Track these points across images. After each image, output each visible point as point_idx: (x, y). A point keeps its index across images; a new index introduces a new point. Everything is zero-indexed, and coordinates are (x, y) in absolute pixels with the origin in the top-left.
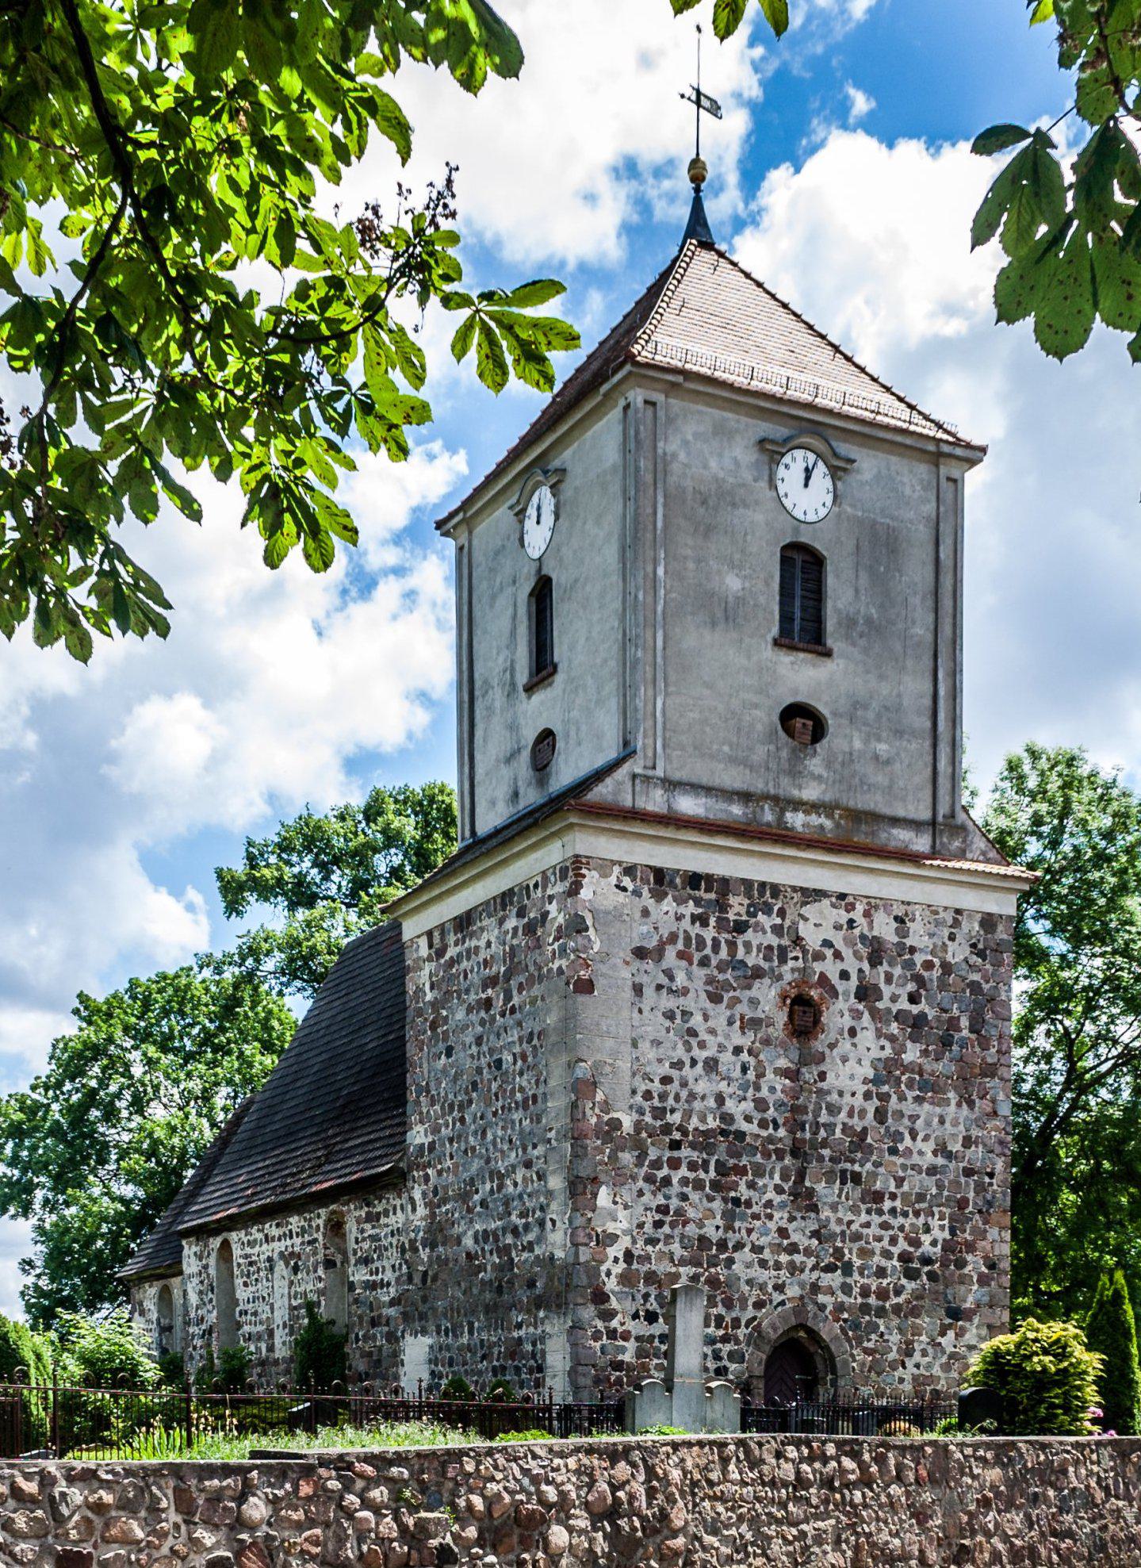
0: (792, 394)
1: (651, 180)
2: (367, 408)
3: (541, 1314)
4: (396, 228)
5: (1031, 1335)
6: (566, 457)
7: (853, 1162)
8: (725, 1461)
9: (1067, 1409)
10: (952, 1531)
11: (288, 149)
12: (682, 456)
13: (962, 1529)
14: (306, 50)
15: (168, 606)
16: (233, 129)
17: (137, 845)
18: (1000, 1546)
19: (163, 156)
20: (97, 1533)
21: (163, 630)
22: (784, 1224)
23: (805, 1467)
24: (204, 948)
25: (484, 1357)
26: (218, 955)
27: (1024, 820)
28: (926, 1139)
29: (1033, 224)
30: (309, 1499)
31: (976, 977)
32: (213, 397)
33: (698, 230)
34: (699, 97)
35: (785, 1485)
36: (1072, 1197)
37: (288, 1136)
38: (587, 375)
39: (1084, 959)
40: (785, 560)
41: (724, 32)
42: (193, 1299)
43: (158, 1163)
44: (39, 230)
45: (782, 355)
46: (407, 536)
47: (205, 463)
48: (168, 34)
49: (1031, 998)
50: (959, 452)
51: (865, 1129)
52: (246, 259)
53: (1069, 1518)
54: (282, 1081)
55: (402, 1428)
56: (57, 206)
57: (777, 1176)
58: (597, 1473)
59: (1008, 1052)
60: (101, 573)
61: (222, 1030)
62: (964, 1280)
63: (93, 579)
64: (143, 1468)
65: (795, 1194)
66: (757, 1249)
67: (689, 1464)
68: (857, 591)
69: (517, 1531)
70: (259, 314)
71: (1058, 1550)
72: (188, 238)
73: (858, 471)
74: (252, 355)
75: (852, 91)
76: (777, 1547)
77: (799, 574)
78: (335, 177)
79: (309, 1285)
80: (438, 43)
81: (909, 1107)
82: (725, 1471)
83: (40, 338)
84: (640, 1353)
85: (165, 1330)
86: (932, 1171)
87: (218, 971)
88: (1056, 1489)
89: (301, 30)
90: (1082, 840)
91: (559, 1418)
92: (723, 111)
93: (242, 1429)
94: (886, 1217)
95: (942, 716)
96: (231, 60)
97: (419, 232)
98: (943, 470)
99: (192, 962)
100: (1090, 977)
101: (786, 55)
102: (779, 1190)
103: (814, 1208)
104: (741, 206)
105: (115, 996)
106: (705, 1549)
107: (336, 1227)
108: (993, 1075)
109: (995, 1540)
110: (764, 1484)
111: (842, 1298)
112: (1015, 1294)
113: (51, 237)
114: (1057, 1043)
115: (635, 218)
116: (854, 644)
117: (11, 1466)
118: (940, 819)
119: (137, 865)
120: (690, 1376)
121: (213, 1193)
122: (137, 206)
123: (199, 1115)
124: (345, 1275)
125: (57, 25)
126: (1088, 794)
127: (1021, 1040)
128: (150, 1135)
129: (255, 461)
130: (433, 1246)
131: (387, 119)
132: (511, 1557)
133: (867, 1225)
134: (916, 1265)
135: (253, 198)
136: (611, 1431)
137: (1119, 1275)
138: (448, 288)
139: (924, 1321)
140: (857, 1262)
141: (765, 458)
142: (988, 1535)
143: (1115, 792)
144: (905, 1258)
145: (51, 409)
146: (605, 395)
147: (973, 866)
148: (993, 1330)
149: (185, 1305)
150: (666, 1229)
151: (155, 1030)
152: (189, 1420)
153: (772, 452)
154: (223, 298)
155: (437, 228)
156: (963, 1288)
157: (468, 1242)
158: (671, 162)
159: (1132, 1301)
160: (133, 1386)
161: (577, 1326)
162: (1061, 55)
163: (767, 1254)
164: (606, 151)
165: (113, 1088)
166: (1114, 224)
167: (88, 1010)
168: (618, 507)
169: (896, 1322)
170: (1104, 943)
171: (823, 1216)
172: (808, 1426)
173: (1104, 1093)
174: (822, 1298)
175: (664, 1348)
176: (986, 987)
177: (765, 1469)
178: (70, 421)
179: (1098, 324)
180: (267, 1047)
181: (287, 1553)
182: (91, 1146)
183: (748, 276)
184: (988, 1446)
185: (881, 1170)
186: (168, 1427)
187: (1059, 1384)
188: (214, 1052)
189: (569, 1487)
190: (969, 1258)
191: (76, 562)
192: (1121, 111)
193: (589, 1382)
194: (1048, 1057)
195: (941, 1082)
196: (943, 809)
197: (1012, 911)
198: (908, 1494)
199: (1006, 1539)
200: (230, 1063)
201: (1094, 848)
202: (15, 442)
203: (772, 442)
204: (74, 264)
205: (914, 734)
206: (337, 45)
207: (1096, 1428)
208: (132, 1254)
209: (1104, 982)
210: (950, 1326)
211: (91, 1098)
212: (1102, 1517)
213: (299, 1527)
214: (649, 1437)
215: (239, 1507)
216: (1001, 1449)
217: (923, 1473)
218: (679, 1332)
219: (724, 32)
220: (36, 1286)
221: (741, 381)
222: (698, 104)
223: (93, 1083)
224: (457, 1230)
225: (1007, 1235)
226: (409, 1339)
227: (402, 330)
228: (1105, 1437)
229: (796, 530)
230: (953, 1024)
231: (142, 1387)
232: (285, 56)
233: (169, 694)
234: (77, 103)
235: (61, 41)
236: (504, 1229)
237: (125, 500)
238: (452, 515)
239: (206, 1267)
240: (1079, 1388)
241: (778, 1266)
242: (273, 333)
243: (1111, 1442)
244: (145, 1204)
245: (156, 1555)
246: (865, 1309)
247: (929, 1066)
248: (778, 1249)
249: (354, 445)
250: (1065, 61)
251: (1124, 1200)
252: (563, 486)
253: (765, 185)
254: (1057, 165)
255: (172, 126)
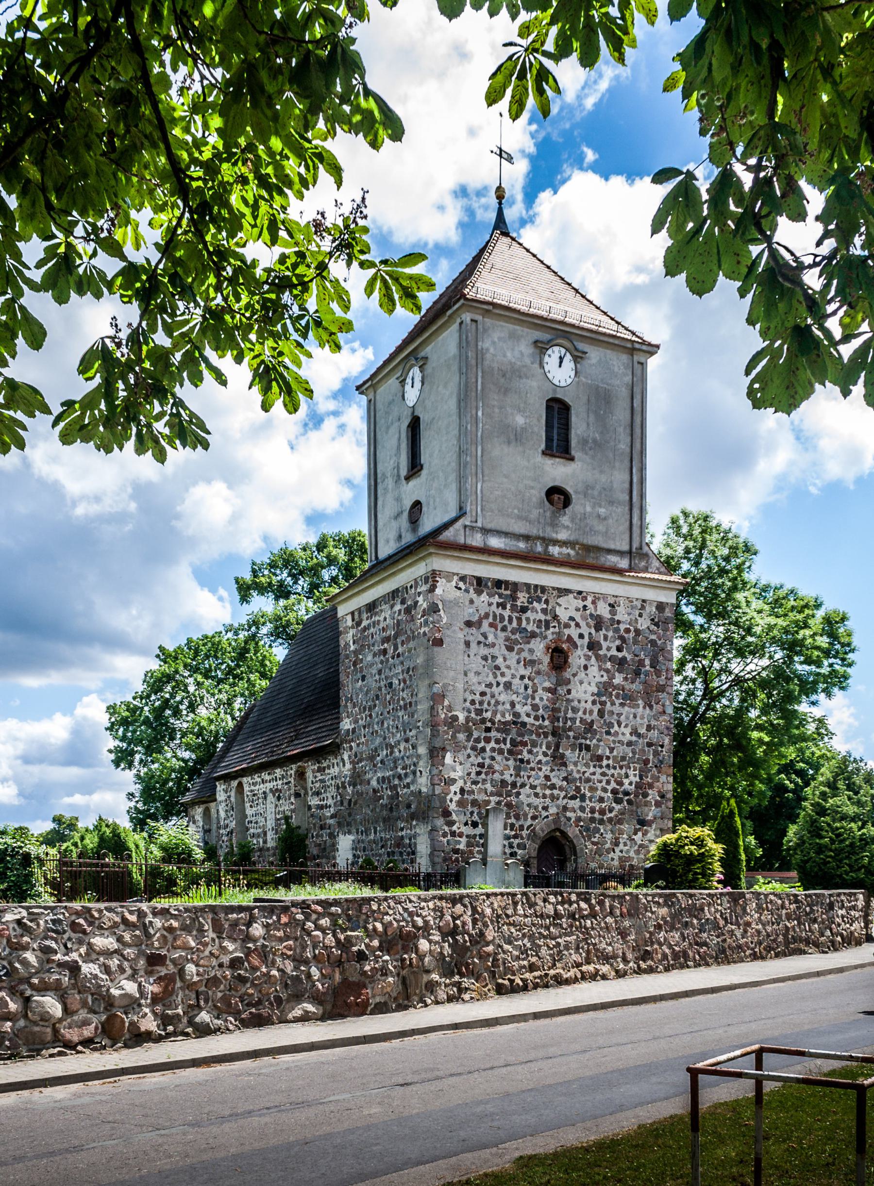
0: (552, 316)
1: (475, 198)
2: (318, 324)
3: (414, 823)
4: (334, 225)
5: (684, 834)
6: (428, 351)
7: (586, 739)
8: (515, 904)
9: (704, 875)
10: (640, 942)
11: (275, 181)
12: (492, 350)
13: (646, 941)
14: (285, 126)
15: (208, 433)
16: (244, 170)
17: (191, 564)
18: (667, 951)
19: (206, 185)
20: (169, 944)
21: (206, 446)
22: (548, 773)
23: (559, 907)
24: (228, 621)
25: (382, 847)
26: (236, 625)
27: (680, 551)
28: (626, 726)
29: (685, 222)
30: (286, 924)
31: (654, 637)
32: (233, 318)
33: (501, 226)
34: (501, 153)
35: (549, 917)
36: (707, 758)
37: (275, 725)
38: (439, 306)
39: (713, 627)
40: (548, 408)
41: (515, 116)
42: (222, 814)
43: (203, 740)
44: (137, 226)
45: (547, 294)
46: (340, 394)
47: (229, 353)
48: (209, 118)
49: (684, 648)
50: (644, 348)
51: (592, 721)
52: (251, 242)
53: (705, 935)
54: (272, 694)
55: (337, 886)
56: (147, 212)
57: (544, 747)
58: (445, 910)
59: (671, 678)
60: (171, 415)
61: (238, 666)
62: (648, 804)
63: (167, 418)
64: (195, 907)
65: (554, 757)
66: (533, 787)
67: (496, 905)
68: (588, 424)
69: (401, 942)
70: (259, 272)
71: (699, 953)
72: (219, 230)
73: (589, 358)
74: (254, 294)
75: (585, 149)
76: (544, 951)
77: (556, 415)
78: (301, 197)
79: (286, 807)
80: (357, 122)
81: (617, 709)
82: (515, 909)
83: (138, 285)
84: (469, 844)
85: (207, 831)
86: (630, 744)
87: (236, 634)
88: (698, 919)
89: (281, 115)
90: (712, 562)
91: (424, 880)
92: (514, 160)
93: (249, 886)
94: (604, 770)
95: (635, 493)
96: (243, 132)
97: (347, 227)
98: (636, 358)
99: (222, 629)
100: (717, 637)
101: (549, 129)
102: (545, 754)
103: (565, 764)
104: (524, 212)
105: (179, 648)
106: (504, 952)
107: (301, 775)
108: (663, 691)
109: (664, 947)
110: (537, 916)
111: (580, 814)
112: (675, 812)
113: (144, 229)
114: (699, 673)
115: (466, 219)
116: (586, 454)
117: (122, 907)
118: (634, 550)
119: (191, 576)
120: (496, 857)
121: (234, 756)
122: (191, 212)
123: (226, 713)
124: (306, 801)
125: (147, 112)
126: (715, 536)
127: (678, 672)
128: (199, 724)
129: (256, 353)
130: (354, 785)
131: (329, 165)
132: (398, 957)
133: (594, 774)
134: (620, 796)
135: (255, 207)
136: (453, 887)
137: (733, 802)
138: (363, 257)
139: (625, 827)
140: (588, 794)
141: (538, 351)
142: (660, 944)
143: (730, 535)
144: (614, 792)
145: (144, 324)
146: (450, 316)
147: (652, 576)
148: (663, 832)
149: (218, 818)
150: (483, 776)
151: (201, 666)
152: (220, 881)
153: (541, 348)
154: (239, 263)
155: (357, 224)
156: (646, 809)
157: (374, 783)
158: (486, 188)
159: (740, 815)
160: (189, 863)
161: (434, 830)
162: (701, 129)
163: (538, 790)
164: (449, 182)
165: (178, 698)
166: (730, 222)
167: (164, 655)
168: (456, 378)
169: (609, 827)
170: (724, 619)
171: (569, 769)
172: (561, 885)
173: (724, 701)
174: (568, 814)
175: (482, 841)
176: (659, 642)
177: (538, 908)
178: (155, 331)
179: (721, 277)
180: (263, 676)
181: (274, 954)
182: (166, 730)
183: (528, 251)
184: (660, 896)
185: (602, 743)
186: (208, 885)
187: (700, 861)
188: (234, 678)
189: (429, 918)
190: (650, 792)
191: (157, 409)
192: (734, 160)
193: (440, 860)
194: (693, 681)
195: (635, 694)
196: (635, 545)
197: (674, 601)
198: (616, 922)
199: (670, 947)
200: (243, 684)
201: (719, 566)
202: (124, 342)
203: (542, 342)
204: (157, 245)
205: (619, 503)
206: (301, 123)
207: (720, 886)
208: (188, 790)
209: (724, 640)
210: (639, 830)
211: (166, 703)
212: (723, 934)
213: (281, 940)
214: (474, 890)
215: (247, 929)
216: (667, 897)
217: (625, 910)
218: (490, 833)
219: (515, 116)
220: (136, 808)
221: (524, 309)
222: (501, 156)
223: (167, 696)
224: (368, 776)
225: (671, 779)
226: (341, 836)
227: (337, 280)
228: (725, 890)
229: (555, 391)
230: (641, 663)
231: (194, 863)
232: (273, 129)
233: (209, 481)
234: (158, 156)
235: (150, 121)
236: (394, 776)
237: (185, 374)
238: (365, 383)
239: (229, 797)
240: (711, 864)
241: (544, 796)
242: (266, 282)
243: (728, 893)
244: (196, 762)
245: (202, 955)
246: (592, 820)
247: (628, 686)
248: (545, 787)
249: (311, 344)
250: (703, 132)
251: (735, 760)
252: (426, 367)
253: (538, 201)
254: (698, 190)
255: (211, 169)
